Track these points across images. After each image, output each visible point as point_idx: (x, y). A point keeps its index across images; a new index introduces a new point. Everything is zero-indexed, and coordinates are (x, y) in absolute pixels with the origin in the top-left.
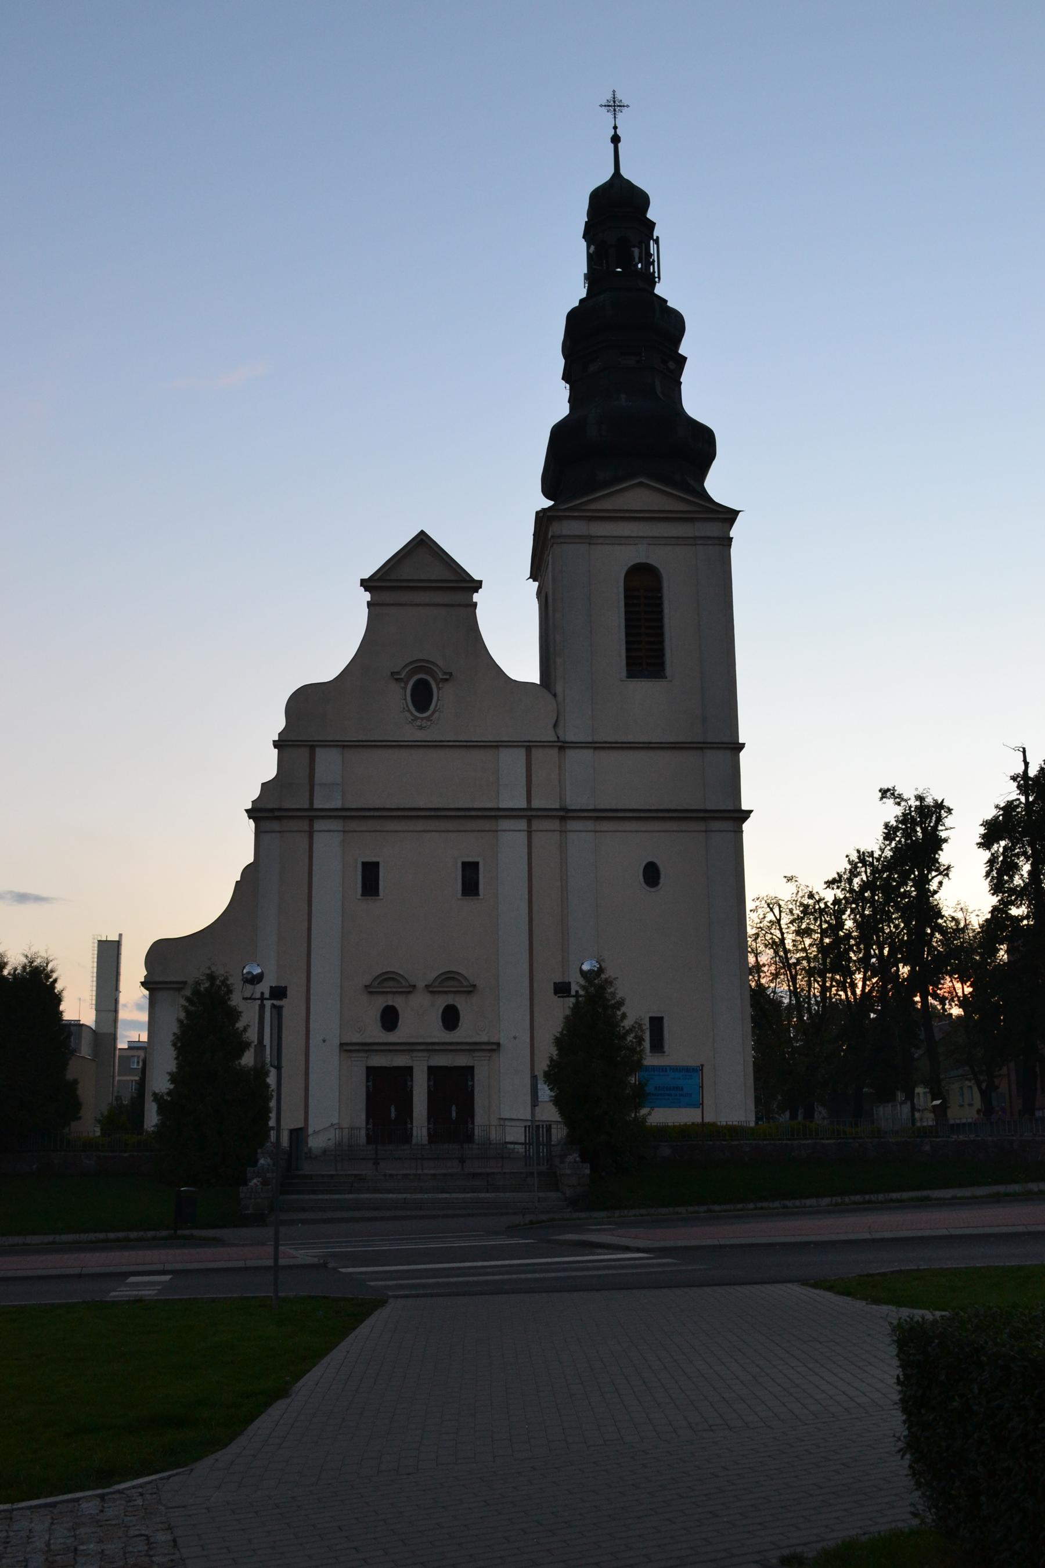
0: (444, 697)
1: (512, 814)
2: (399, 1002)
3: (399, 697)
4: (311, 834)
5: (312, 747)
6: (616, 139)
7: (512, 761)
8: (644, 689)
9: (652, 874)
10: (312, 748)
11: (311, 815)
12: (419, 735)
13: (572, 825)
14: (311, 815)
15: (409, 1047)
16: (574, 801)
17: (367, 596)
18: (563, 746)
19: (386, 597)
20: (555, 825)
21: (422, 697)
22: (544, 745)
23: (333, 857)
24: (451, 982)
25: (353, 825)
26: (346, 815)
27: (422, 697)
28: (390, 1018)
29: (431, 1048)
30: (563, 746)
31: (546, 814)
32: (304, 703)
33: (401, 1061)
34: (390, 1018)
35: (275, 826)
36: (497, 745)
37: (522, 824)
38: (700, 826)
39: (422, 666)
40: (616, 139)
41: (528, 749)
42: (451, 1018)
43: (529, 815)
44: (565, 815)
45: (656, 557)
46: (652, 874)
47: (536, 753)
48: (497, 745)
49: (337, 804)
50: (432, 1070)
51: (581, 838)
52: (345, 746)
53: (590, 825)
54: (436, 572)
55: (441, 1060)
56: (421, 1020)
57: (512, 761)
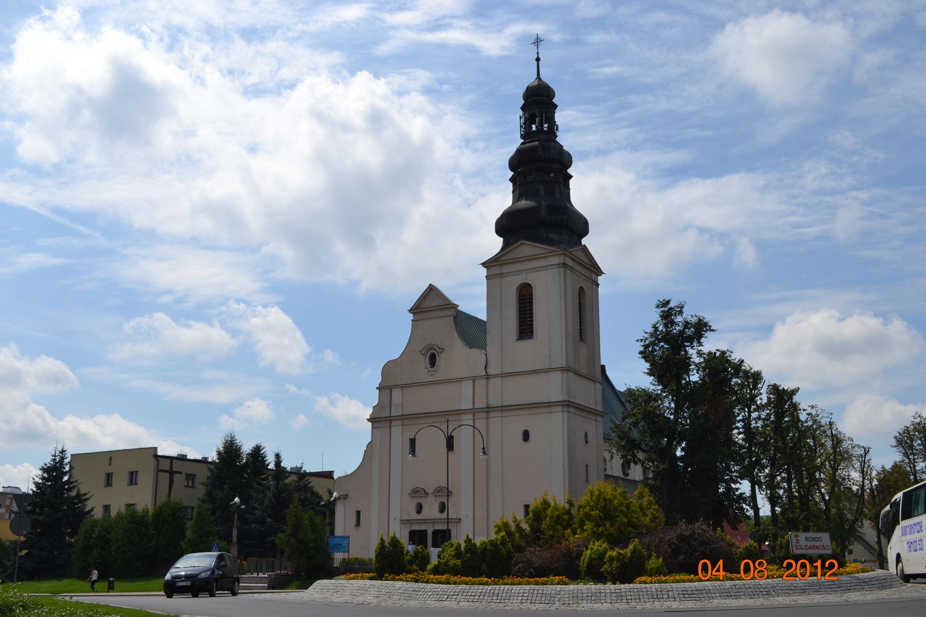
0: (441, 360)
1: (466, 411)
2: (423, 501)
3: (424, 362)
4: (390, 427)
5: (390, 389)
6: (538, 60)
7: (467, 386)
8: (526, 344)
9: (526, 436)
10: (391, 390)
11: (390, 419)
12: (431, 379)
13: (492, 415)
14: (390, 419)
15: (425, 521)
16: (494, 402)
17: (411, 316)
18: (488, 377)
19: (419, 316)
20: (484, 415)
21: (433, 360)
22: (480, 377)
23: (399, 436)
24: (438, 490)
25: (406, 422)
26: (404, 418)
27: (433, 360)
28: (419, 509)
29: (434, 521)
30: (488, 377)
31: (480, 410)
32: (389, 369)
33: (423, 528)
34: (419, 509)
35: (378, 425)
36: (460, 380)
37: (471, 416)
38: (547, 410)
39: (430, 347)
40: (538, 60)
41: (474, 381)
42: (443, 508)
43: (474, 411)
44: (488, 409)
45: (530, 279)
46: (526, 436)
47: (477, 382)
48: (460, 380)
49: (400, 414)
50: (435, 532)
51: (496, 420)
52: (403, 387)
53: (499, 414)
54: (437, 302)
55: (439, 527)
56: (431, 510)
57: (467, 386)
